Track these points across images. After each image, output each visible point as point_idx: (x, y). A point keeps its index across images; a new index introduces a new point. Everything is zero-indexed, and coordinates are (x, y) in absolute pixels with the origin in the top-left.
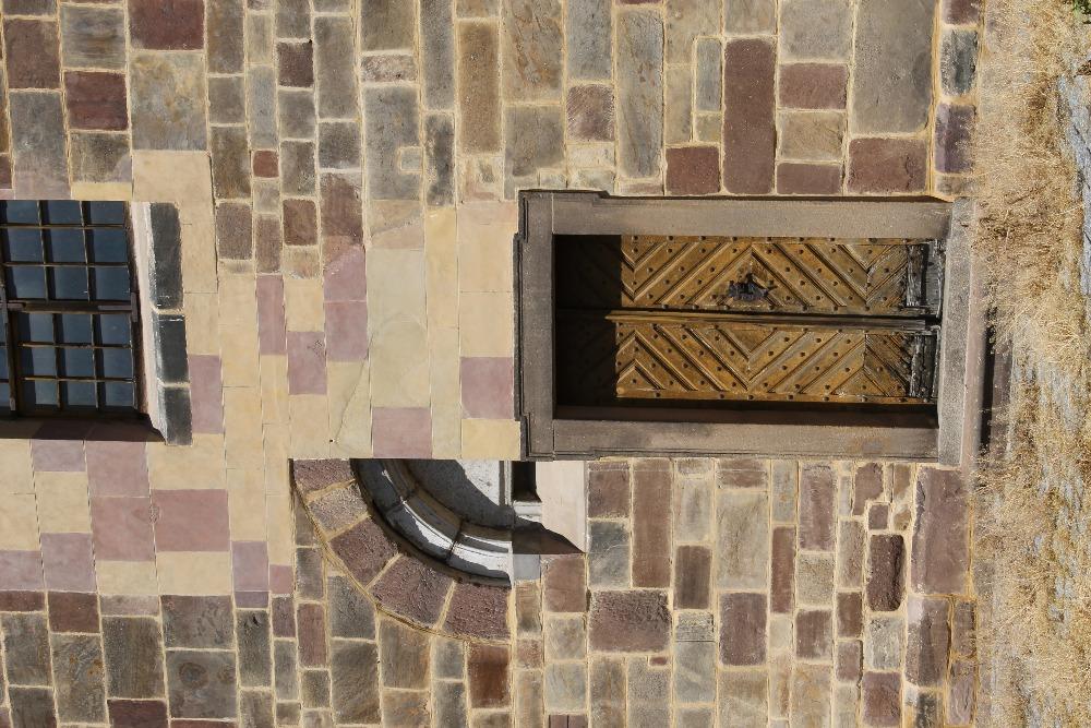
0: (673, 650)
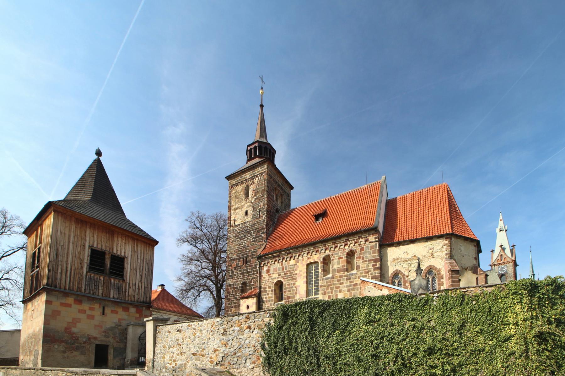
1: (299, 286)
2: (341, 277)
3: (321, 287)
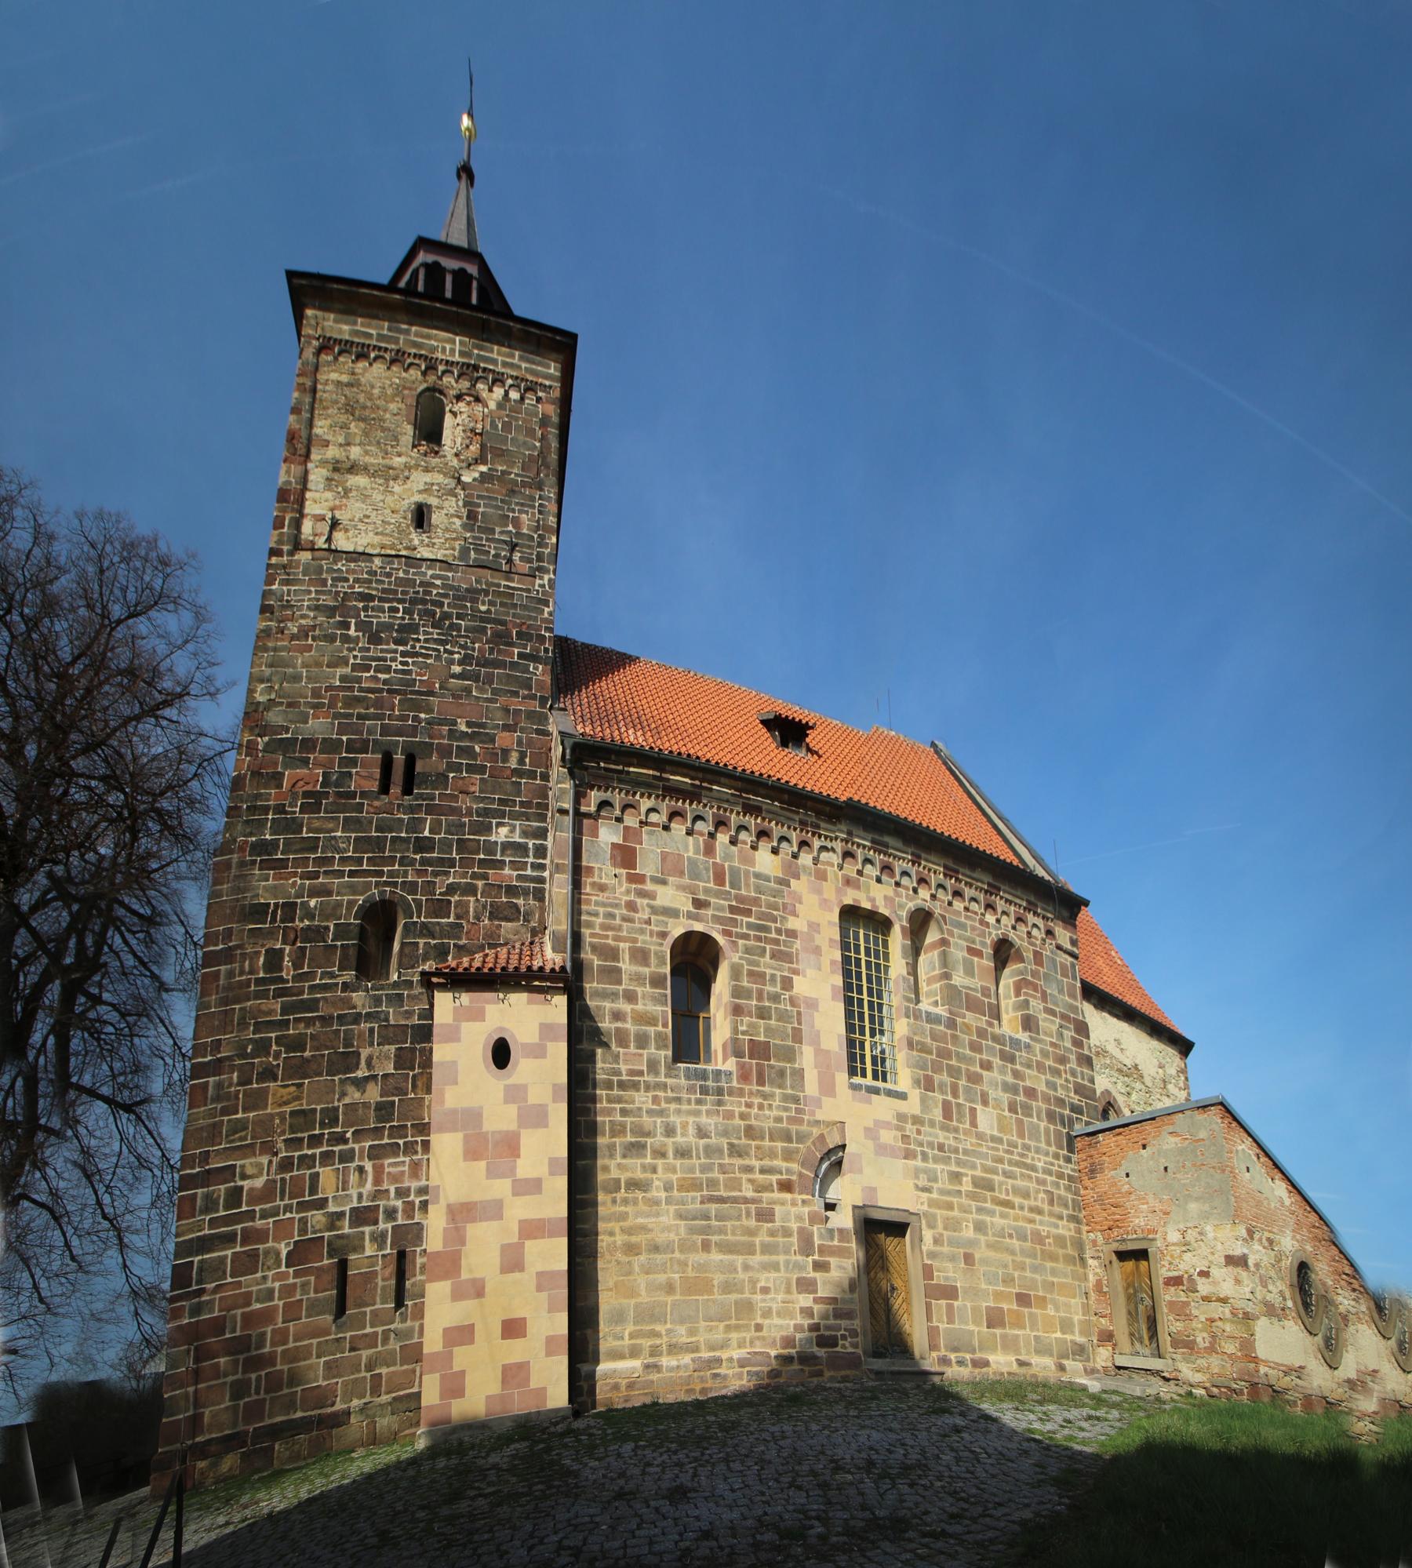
0: (799, 1258)
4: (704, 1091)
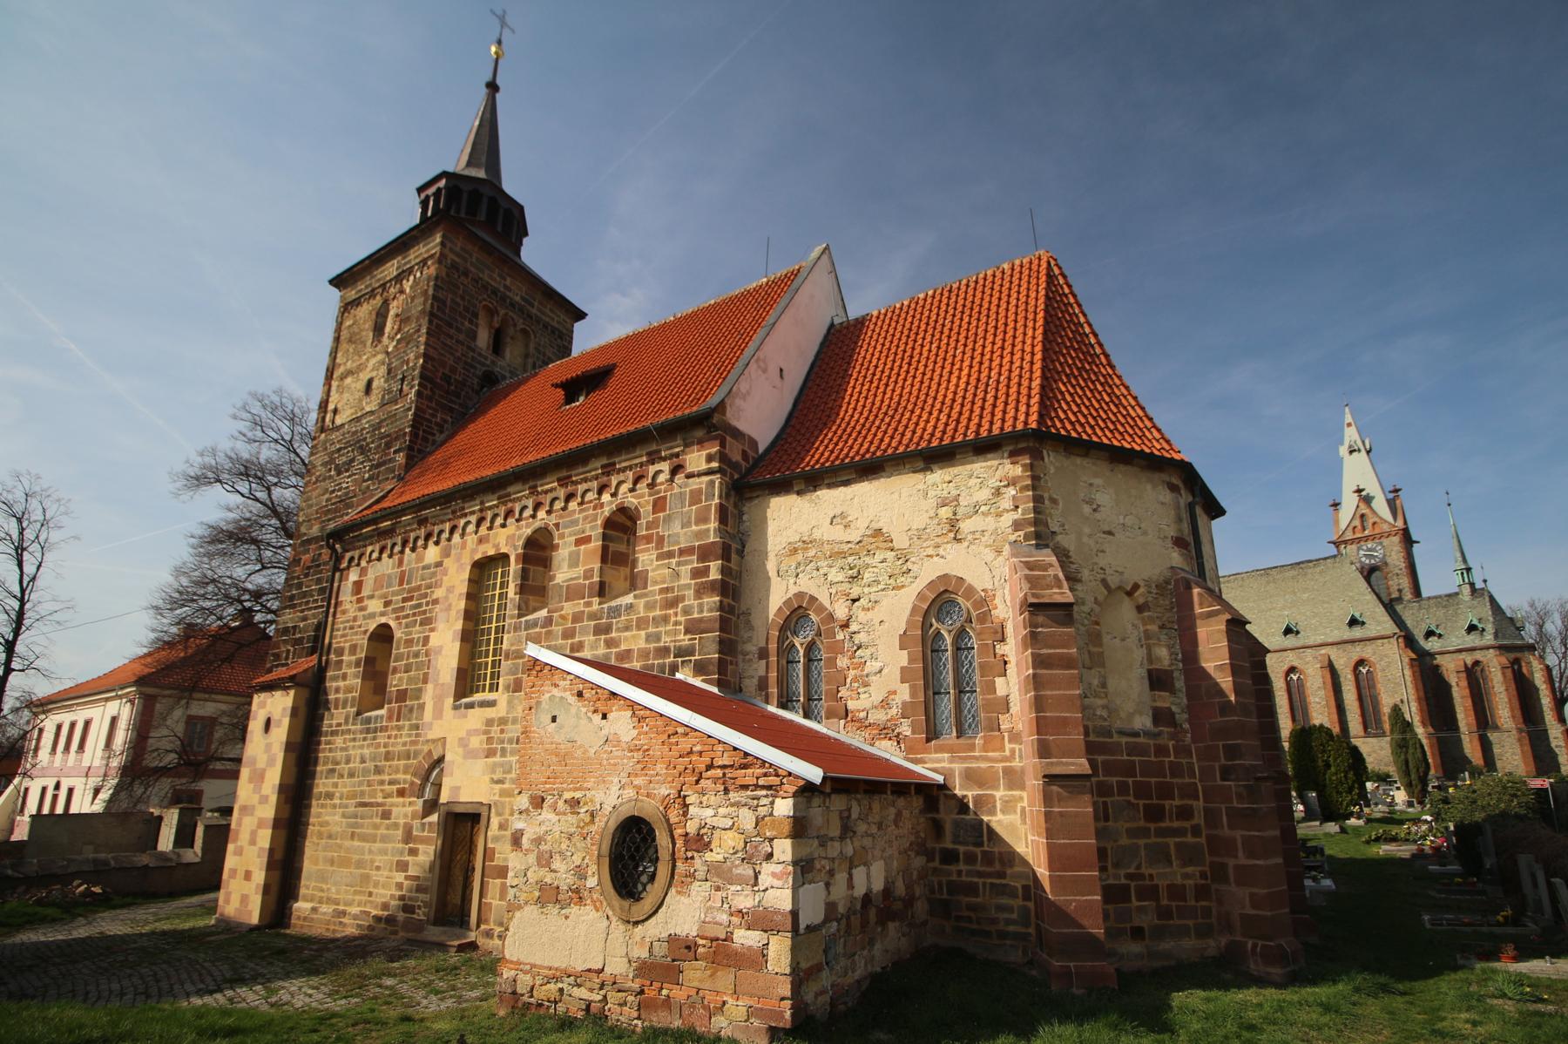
1: (439, 650)
2: (577, 618)
3: (507, 657)
4: (368, 731)
